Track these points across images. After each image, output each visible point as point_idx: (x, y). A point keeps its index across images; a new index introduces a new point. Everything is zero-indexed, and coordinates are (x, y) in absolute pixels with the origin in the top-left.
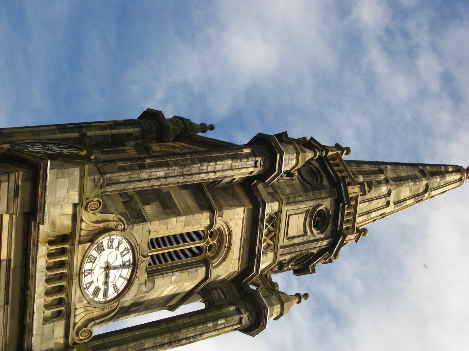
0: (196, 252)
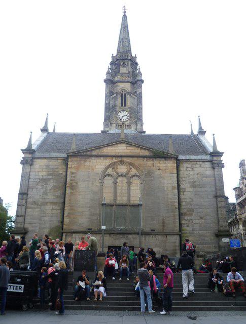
0: (125, 94)
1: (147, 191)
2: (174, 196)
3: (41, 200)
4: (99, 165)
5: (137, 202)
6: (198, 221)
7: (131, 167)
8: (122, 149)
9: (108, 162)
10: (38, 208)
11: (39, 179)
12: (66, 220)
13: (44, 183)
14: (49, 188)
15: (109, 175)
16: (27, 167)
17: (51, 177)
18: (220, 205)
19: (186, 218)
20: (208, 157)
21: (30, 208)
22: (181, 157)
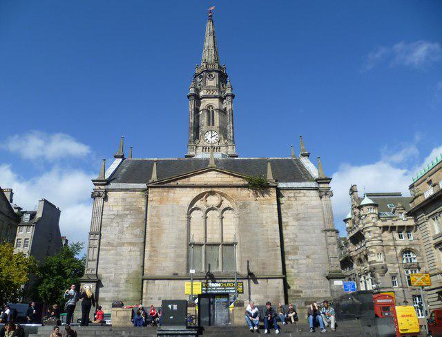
1: (244, 226)
2: (275, 231)
3: (116, 240)
4: (184, 196)
5: (231, 240)
6: (304, 261)
7: (223, 198)
8: (211, 177)
9: (197, 192)
10: (113, 249)
11: (114, 215)
12: (147, 264)
13: (120, 220)
14: (126, 226)
15: (198, 209)
16: (100, 201)
17: (128, 212)
18: (329, 241)
19: (290, 258)
20: (314, 185)
21: (105, 250)
22: (281, 185)
